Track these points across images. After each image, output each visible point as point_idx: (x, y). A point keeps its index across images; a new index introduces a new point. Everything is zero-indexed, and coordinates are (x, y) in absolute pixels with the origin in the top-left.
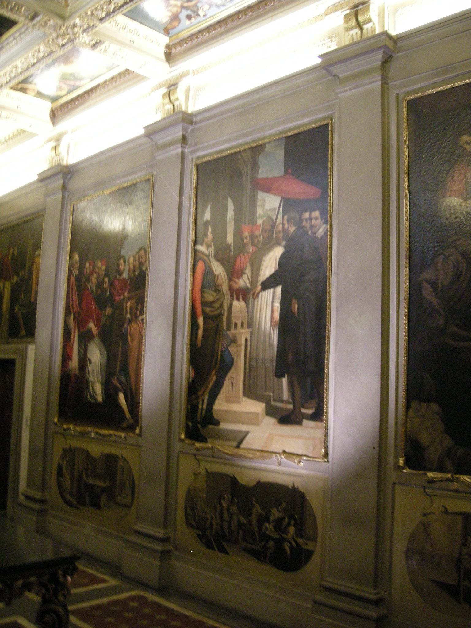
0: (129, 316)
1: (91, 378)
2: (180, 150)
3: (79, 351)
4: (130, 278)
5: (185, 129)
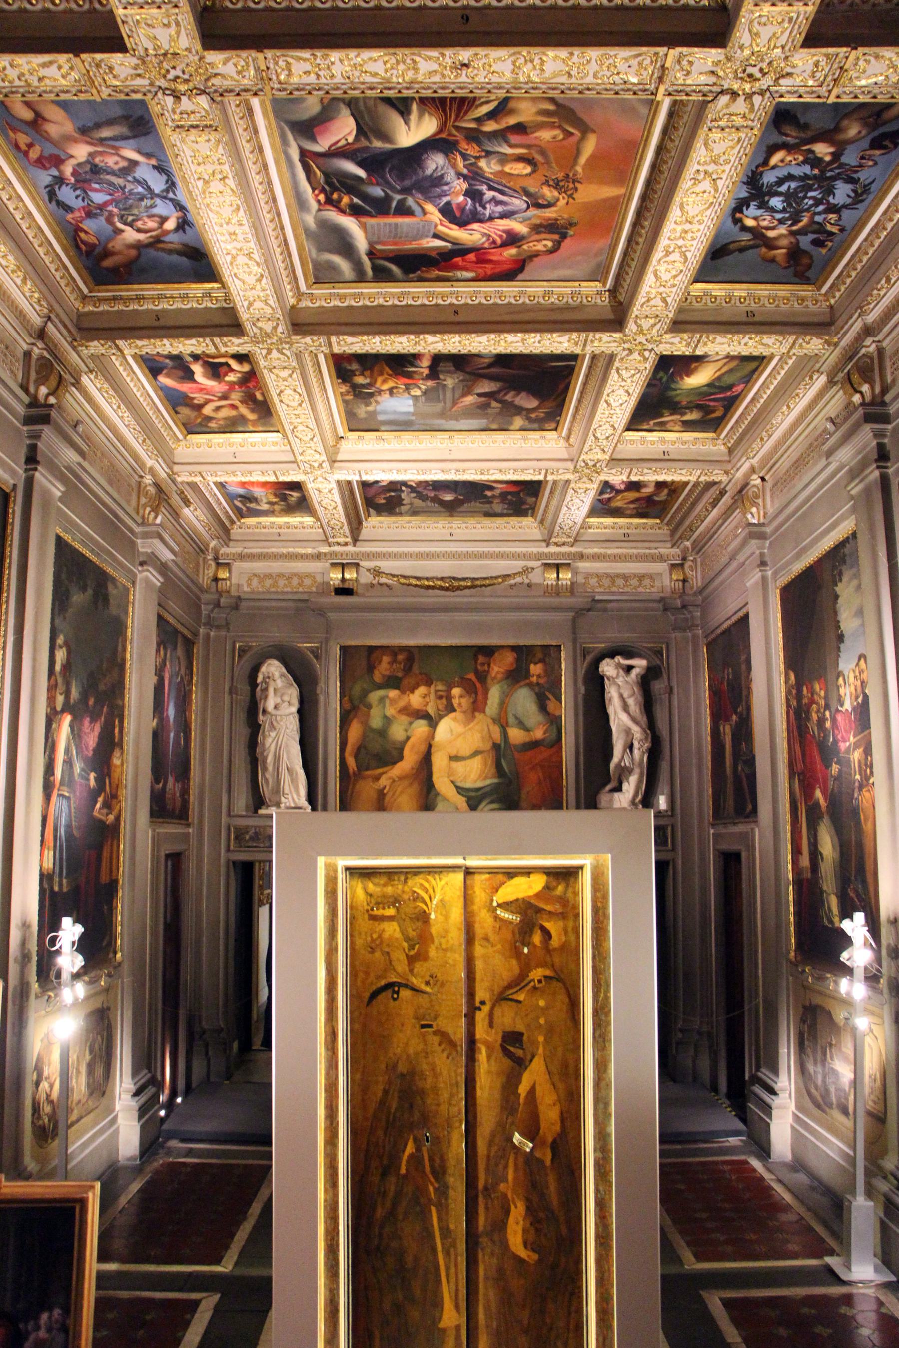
0: (858, 777)
1: (825, 888)
2: (876, 473)
3: (809, 839)
4: (854, 709)
5: (878, 435)
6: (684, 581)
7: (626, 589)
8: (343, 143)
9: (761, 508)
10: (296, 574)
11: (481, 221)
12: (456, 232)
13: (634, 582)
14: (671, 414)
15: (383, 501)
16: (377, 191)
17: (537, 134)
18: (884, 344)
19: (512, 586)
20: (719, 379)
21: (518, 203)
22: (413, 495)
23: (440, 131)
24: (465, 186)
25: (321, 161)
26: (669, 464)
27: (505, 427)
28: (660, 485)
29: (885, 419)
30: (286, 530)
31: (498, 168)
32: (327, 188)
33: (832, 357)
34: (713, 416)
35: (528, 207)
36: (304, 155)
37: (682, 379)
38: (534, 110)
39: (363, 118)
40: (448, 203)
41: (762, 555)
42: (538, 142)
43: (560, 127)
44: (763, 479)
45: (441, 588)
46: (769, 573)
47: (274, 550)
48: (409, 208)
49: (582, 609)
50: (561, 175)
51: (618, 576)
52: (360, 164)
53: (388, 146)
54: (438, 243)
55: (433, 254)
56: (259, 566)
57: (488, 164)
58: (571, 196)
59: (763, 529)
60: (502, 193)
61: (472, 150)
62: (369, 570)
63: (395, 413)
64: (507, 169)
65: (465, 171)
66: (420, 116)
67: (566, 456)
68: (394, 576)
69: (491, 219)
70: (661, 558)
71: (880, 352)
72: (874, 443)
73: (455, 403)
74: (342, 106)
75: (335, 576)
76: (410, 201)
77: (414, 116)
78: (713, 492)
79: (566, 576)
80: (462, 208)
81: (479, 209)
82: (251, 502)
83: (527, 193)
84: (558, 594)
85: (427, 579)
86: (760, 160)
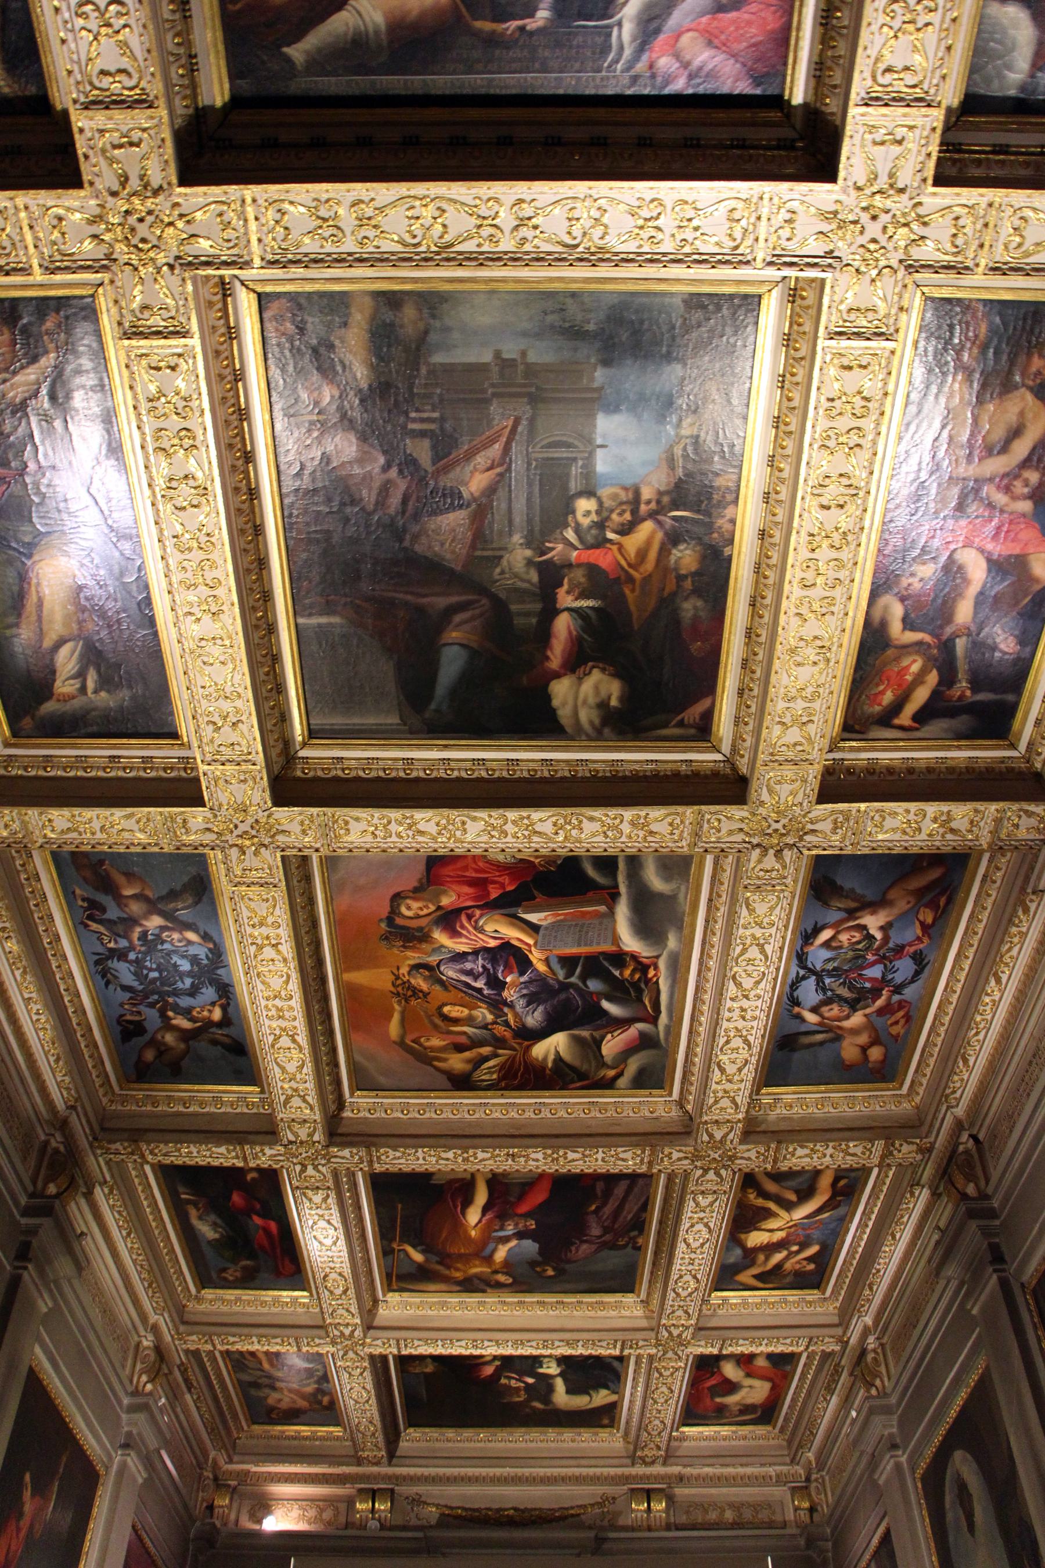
12: (513, 934)
16: (594, 985)
21: (450, 972)
23: (528, 1048)
25: (640, 1014)
31: (475, 1013)
32: (643, 986)
35: (438, 965)
36: (654, 1020)
38: (451, 1062)
40: (522, 973)
43: (425, 1048)
48: (562, 967)
50: (413, 1002)
52: (605, 1013)
53: (576, 1032)
54: (533, 918)
55: (540, 898)
57: (484, 1017)
60: (467, 985)
61: (500, 1030)
64: (466, 1012)
65: (506, 1010)
66: (545, 1058)
69: (476, 953)
76: (561, 974)
77: (551, 1057)
80: (508, 969)
81: (489, 966)
83: (442, 983)
86: (230, 1010)
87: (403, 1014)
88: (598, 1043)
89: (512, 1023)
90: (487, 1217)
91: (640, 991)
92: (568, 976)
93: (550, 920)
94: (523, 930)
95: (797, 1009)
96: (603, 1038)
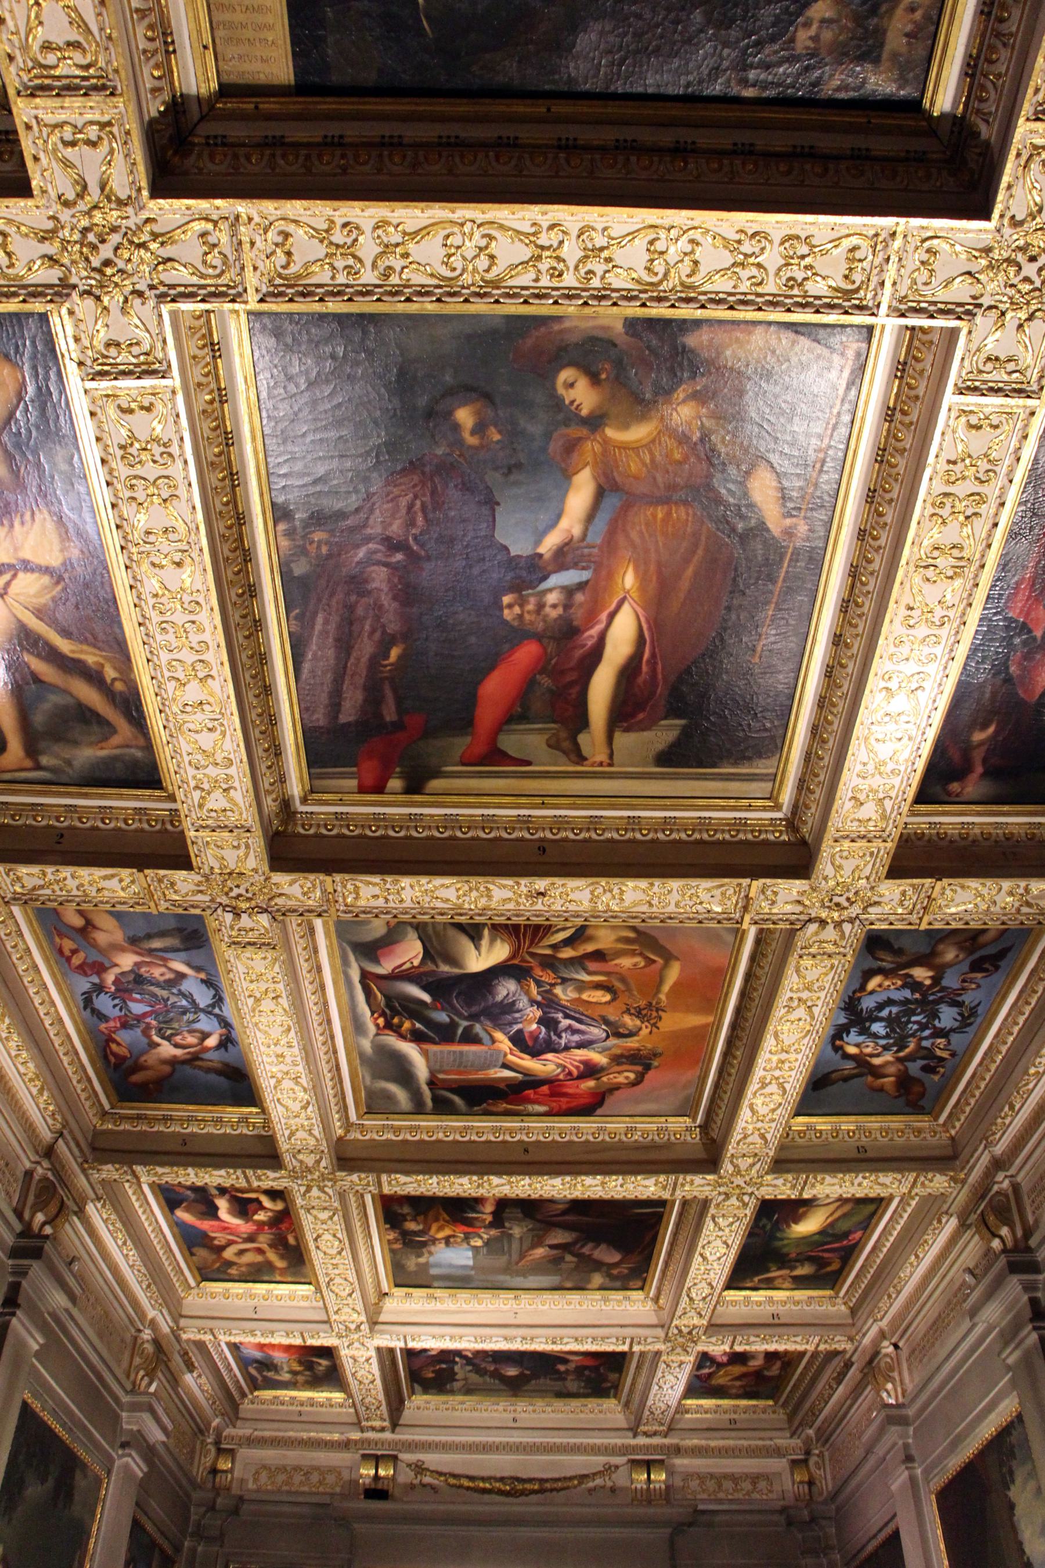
5: (1029, 1287)
6: (811, 1483)
7: (737, 1496)
8: (408, 965)
9: (898, 1383)
10: (317, 1468)
11: (555, 1051)
12: (528, 1063)
13: (747, 1485)
14: (779, 1269)
15: (431, 1375)
16: (442, 1017)
17: (617, 961)
18: (1019, 1179)
19: (591, 1491)
20: (832, 1225)
21: (597, 1032)
22: (470, 1368)
23: (514, 955)
24: (539, 1013)
25: (384, 984)
26: (780, 1330)
27: (581, 1285)
28: (771, 1357)
29: (1033, 1268)
30: (309, 1409)
32: (388, 1011)
33: (962, 1196)
34: (829, 1269)
35: (608, 1037)
36: (365, 976)
37: (789, 1226)
39: (430, 941)
40: (520, 1032)
41: (906, 1446)
42: (617, 969)
43: (641, 954)
44: (896, 1346)
45: (501, 1492)
46: (919, 1471)
47: (291, 1434)
48: (477, 1035)
49: (683, 1524)
50: (642, 1003)
51: (726, 1476)
52: (425, 988)
53: (457, 971)
54: (507, 1073)
55: (502, 1086)
56: (269, 1455)
57: (564, 991)
58: (654, 1025)
59: (904, 1412)
61: (547, 977)
62: (409, 1465)
63: (451, 1266)
66: (492, 941)
67: (654, 1321)
68: (440, 1474)
69: (567, 1048)
70: (778, 1452)
71: (1016, 1187)
72: (1025, 1298)
73: (522, 1256)
74: (409, 929)
75: (367, 1471)
76: (478, 1028)
77: (485, 942)
78: (837, 1363)
79: (660, 1477)
80: (535, 1036)
81: (554, 1037)
82: (269, 1370)
83: (607, 1022)
84: (649, 1502)
85: (483, 1479)
86: (857, 986)
87: (658, 991)
88: (427, 955)
89: (533, 985)
90: (594, 631)
91: (388, 1005)
92: (471, 1027)
93: (492, 1071)
94: (518, 1065)
95: (203, 976)
96: (423, 961)
